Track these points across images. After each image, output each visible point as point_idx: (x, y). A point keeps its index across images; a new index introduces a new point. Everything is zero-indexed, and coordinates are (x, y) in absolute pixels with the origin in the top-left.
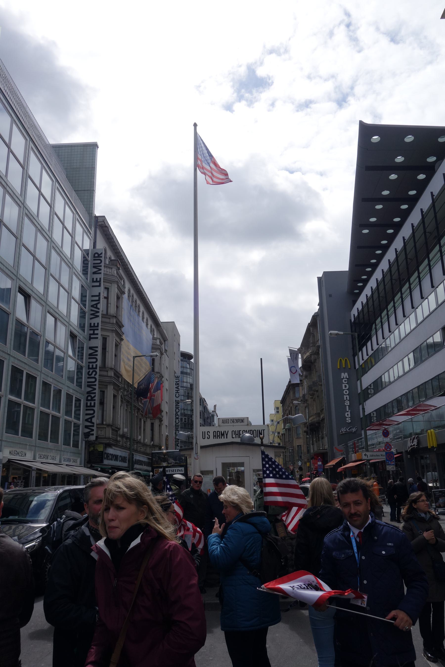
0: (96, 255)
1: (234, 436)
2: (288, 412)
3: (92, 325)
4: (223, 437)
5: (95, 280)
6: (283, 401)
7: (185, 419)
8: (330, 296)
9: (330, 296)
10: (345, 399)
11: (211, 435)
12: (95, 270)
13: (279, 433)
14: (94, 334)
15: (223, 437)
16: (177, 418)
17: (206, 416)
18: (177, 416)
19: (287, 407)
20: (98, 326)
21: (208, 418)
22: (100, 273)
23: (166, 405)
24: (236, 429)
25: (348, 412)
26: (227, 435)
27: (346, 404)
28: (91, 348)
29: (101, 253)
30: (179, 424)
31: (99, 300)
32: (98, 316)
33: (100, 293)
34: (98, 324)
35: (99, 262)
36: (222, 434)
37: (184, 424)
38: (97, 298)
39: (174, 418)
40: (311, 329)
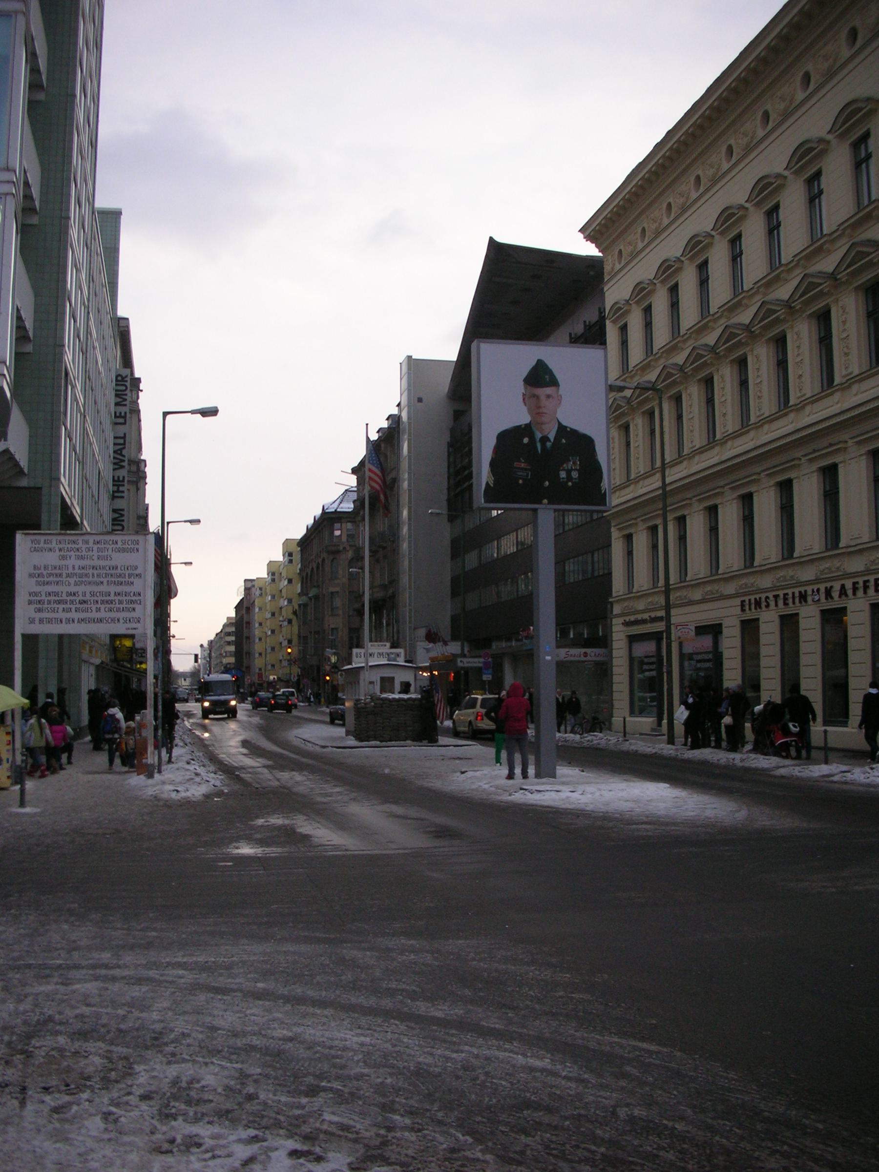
0: (119, 378)
2: (315, 565)
3: (116, 478)
5: (118, 414)
6: (305, 543)
8: (420, 400)
9: (420, 400)
12: (120, 400)
13: (290, 601)
14: (118, 491)
19: (313, 557)
20: (123, 480)
22: (125, 405)
24: (380, 651)
28: (114, 511)
29: (126, 376)
31: (124, 444)
32: (123, 467)
33: (125, 434)
34: (124, 477)
35: (124, 388)
38: (122, 441)
40: (383, 445)
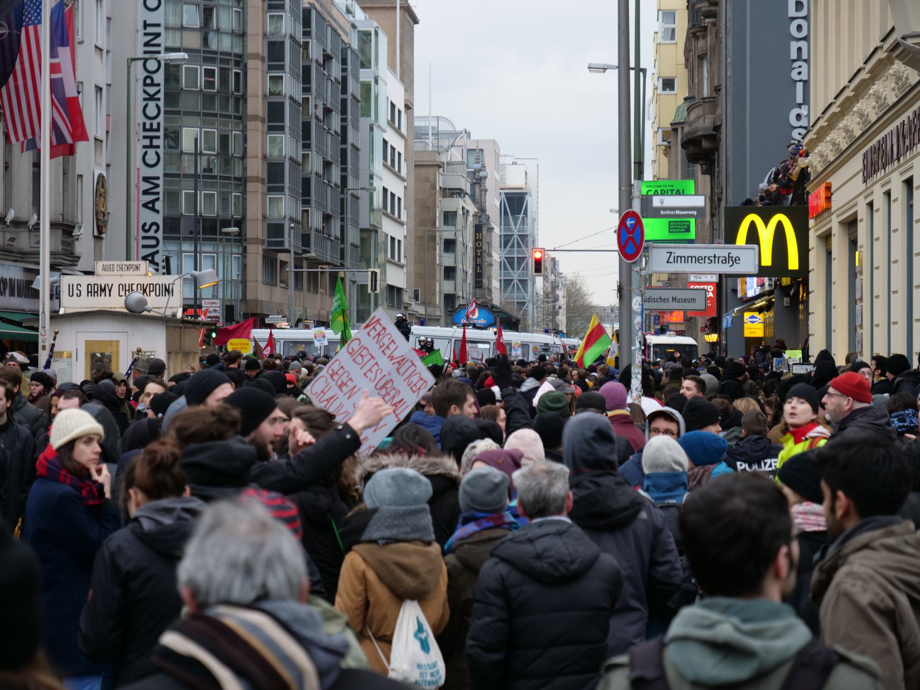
1: (122, 293)
4: (103, 294)
7: (209, 73)
10: (794, 55)
11: (84, 290)
15: (103, 294)
16: (152, 98)
17: (315, 52)
18: (152, 90)
21: (327, 58)
23: (96, 58)
24: (127, 281)
25: (800, 105)
26: (110, 291)
27: (794, 75)
30: (161, 119)
36: (101, 290)
37: (205, 95)
39: (141, 95)
